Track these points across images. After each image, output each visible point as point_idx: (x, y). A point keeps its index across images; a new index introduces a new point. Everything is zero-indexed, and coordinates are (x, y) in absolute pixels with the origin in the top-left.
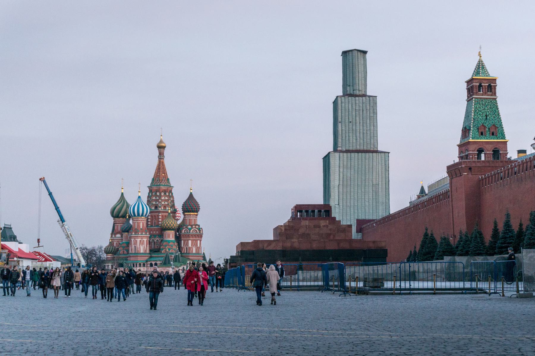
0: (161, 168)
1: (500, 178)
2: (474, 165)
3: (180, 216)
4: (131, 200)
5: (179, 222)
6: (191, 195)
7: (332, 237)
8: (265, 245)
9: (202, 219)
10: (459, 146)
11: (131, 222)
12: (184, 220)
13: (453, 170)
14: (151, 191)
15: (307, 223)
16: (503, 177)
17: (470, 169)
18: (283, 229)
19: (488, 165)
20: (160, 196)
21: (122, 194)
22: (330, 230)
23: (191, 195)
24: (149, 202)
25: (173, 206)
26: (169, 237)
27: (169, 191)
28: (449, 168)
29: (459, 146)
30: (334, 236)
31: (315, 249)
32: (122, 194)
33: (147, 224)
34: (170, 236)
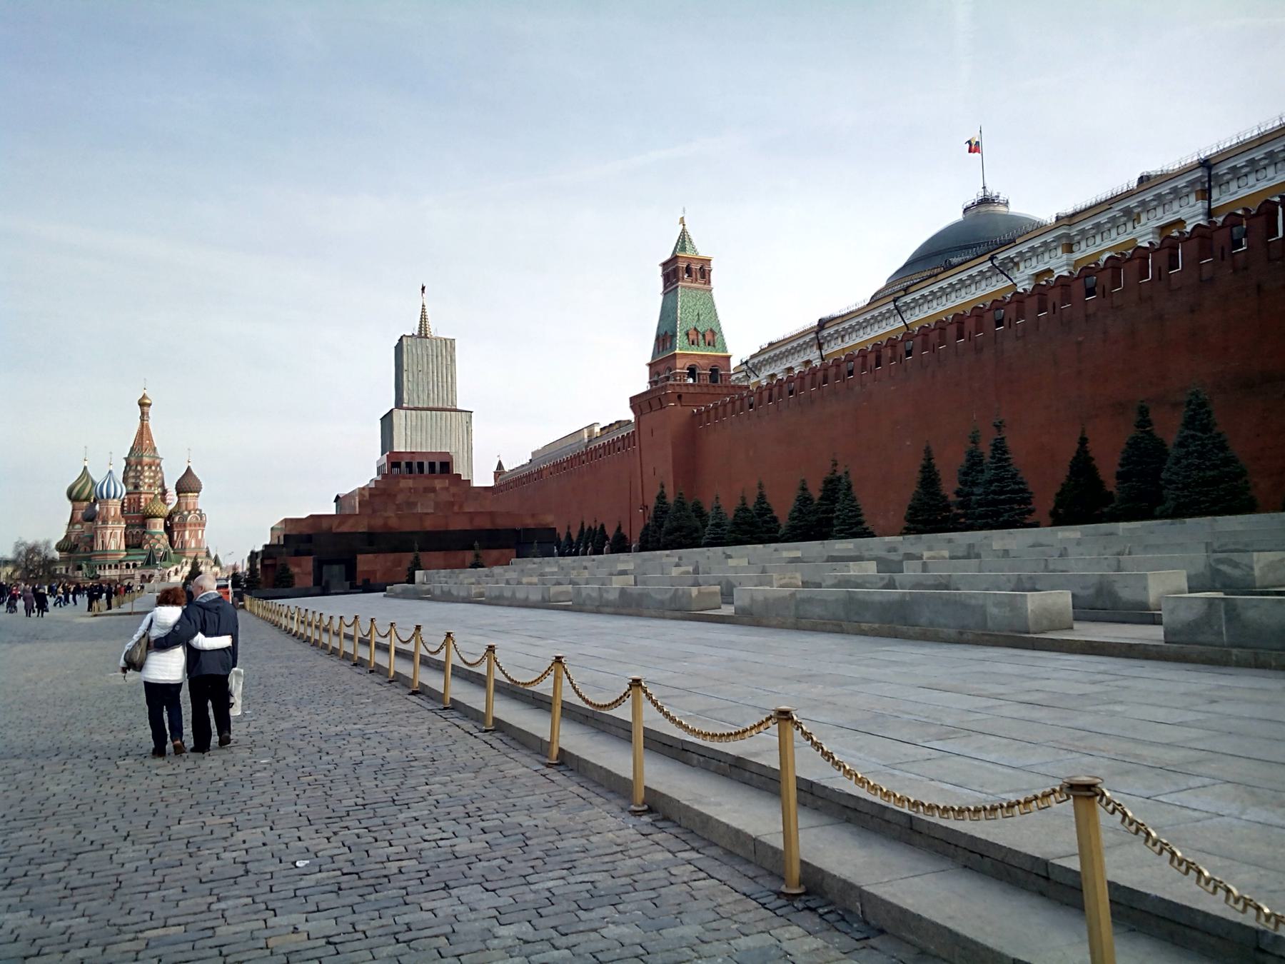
0: (143, 433)
1: (747, 406)
2: (684, 390)
3: (172, 498)
4: (98, 476)
5: (171, 507)
6: (189, 469)
7: (456, 508)
8: (336, 522)
9: (202, 502)
10: (650, 365)
11: (97, 507)
12: (179, 503)
13: (637, 403)
14: (128, 464)
15: (410, 483)
16: (756, 402)
17: (680, 397)
18: (367, 494)
19: (705, 390)
20: (142, 472)
21: (85, 468)
22: (454, 495)
23: (189, 469)
24: (125, 480)
25: (162, 485)
26: (155, 526)
27: (155, 465)
28: (632, 399)
29: (650, 365)
30: (461, 507)
31: (429, 529)
32: (85, 468)
33: (122, 510)
34: (158, 526)
